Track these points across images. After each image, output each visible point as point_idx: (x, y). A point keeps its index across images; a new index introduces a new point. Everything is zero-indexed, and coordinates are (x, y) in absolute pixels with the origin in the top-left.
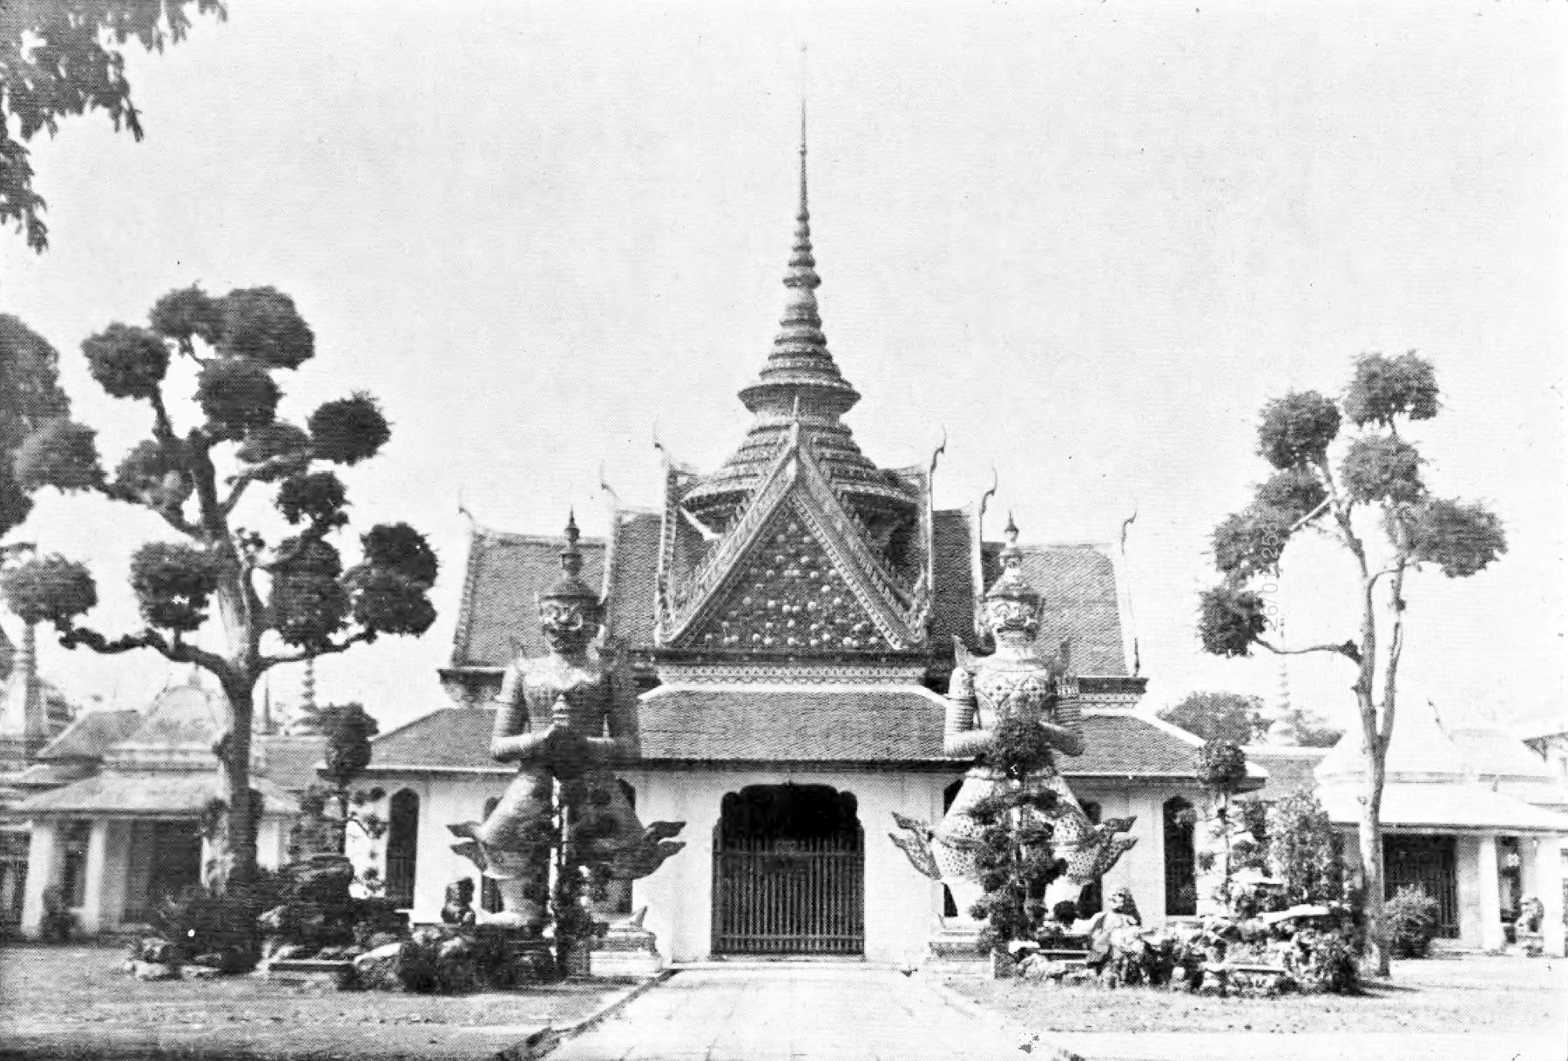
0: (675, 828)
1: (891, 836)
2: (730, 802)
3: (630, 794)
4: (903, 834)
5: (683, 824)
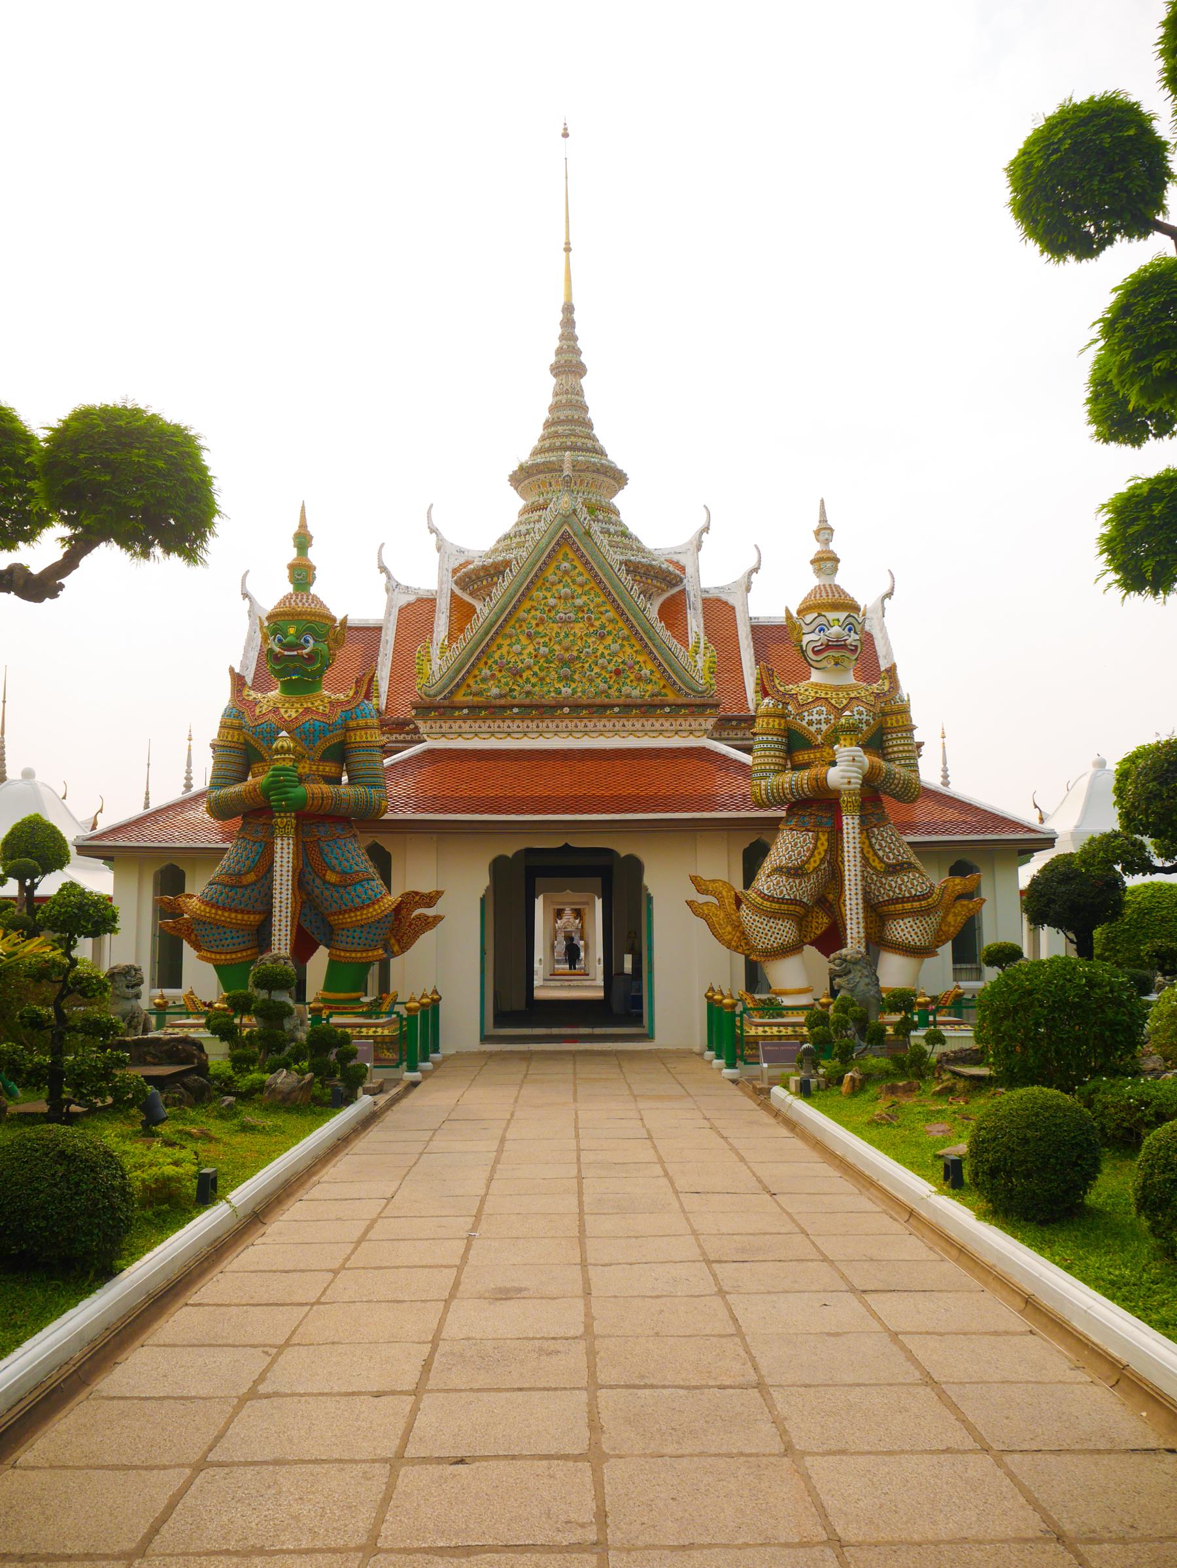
0: (430, 899)
1: (690, 903)
2: (498, 867)
3: (382, 861)
4: (701, 899)
5: (439, 894)
